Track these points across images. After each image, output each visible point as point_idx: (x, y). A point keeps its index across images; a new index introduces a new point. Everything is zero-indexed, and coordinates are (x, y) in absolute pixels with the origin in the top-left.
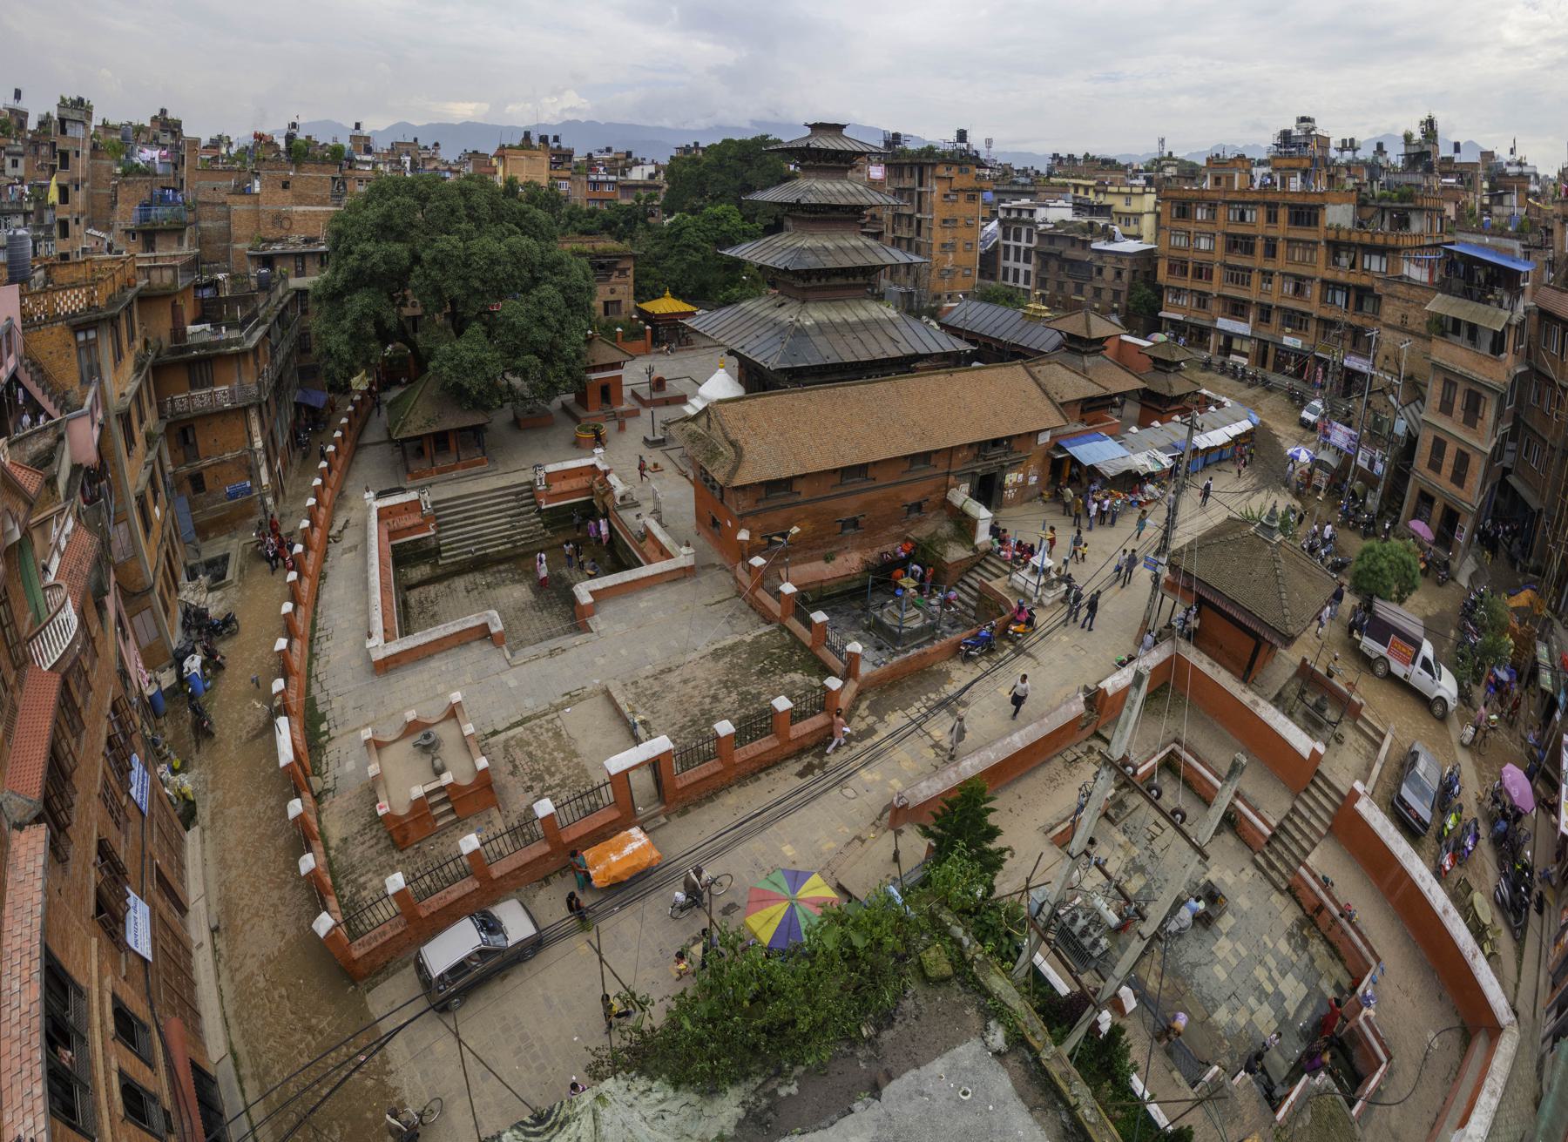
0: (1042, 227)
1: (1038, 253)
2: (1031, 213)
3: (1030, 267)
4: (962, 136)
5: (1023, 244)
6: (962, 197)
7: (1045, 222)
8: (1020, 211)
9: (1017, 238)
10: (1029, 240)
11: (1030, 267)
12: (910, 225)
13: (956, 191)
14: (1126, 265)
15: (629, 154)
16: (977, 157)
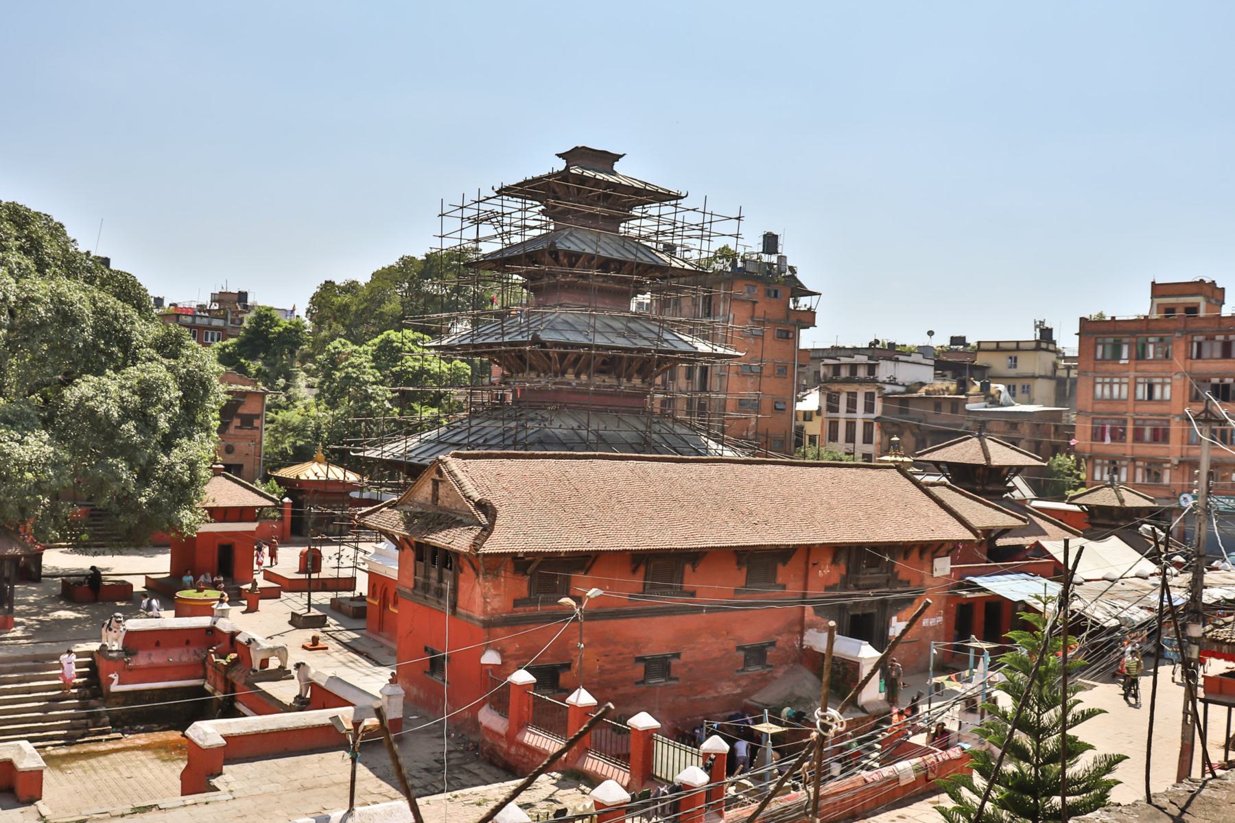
0: (888, 388)
1: (881, 428)
2: (872, 369)
3: (870, 449)
4: (771, 243)
5: (860, 414)
6: (770, 332)
7: (893, 381)
8: (854, 367)
9: (852, 406)
10: (869, 408)
12: (689, 375)
16: (793, 276)
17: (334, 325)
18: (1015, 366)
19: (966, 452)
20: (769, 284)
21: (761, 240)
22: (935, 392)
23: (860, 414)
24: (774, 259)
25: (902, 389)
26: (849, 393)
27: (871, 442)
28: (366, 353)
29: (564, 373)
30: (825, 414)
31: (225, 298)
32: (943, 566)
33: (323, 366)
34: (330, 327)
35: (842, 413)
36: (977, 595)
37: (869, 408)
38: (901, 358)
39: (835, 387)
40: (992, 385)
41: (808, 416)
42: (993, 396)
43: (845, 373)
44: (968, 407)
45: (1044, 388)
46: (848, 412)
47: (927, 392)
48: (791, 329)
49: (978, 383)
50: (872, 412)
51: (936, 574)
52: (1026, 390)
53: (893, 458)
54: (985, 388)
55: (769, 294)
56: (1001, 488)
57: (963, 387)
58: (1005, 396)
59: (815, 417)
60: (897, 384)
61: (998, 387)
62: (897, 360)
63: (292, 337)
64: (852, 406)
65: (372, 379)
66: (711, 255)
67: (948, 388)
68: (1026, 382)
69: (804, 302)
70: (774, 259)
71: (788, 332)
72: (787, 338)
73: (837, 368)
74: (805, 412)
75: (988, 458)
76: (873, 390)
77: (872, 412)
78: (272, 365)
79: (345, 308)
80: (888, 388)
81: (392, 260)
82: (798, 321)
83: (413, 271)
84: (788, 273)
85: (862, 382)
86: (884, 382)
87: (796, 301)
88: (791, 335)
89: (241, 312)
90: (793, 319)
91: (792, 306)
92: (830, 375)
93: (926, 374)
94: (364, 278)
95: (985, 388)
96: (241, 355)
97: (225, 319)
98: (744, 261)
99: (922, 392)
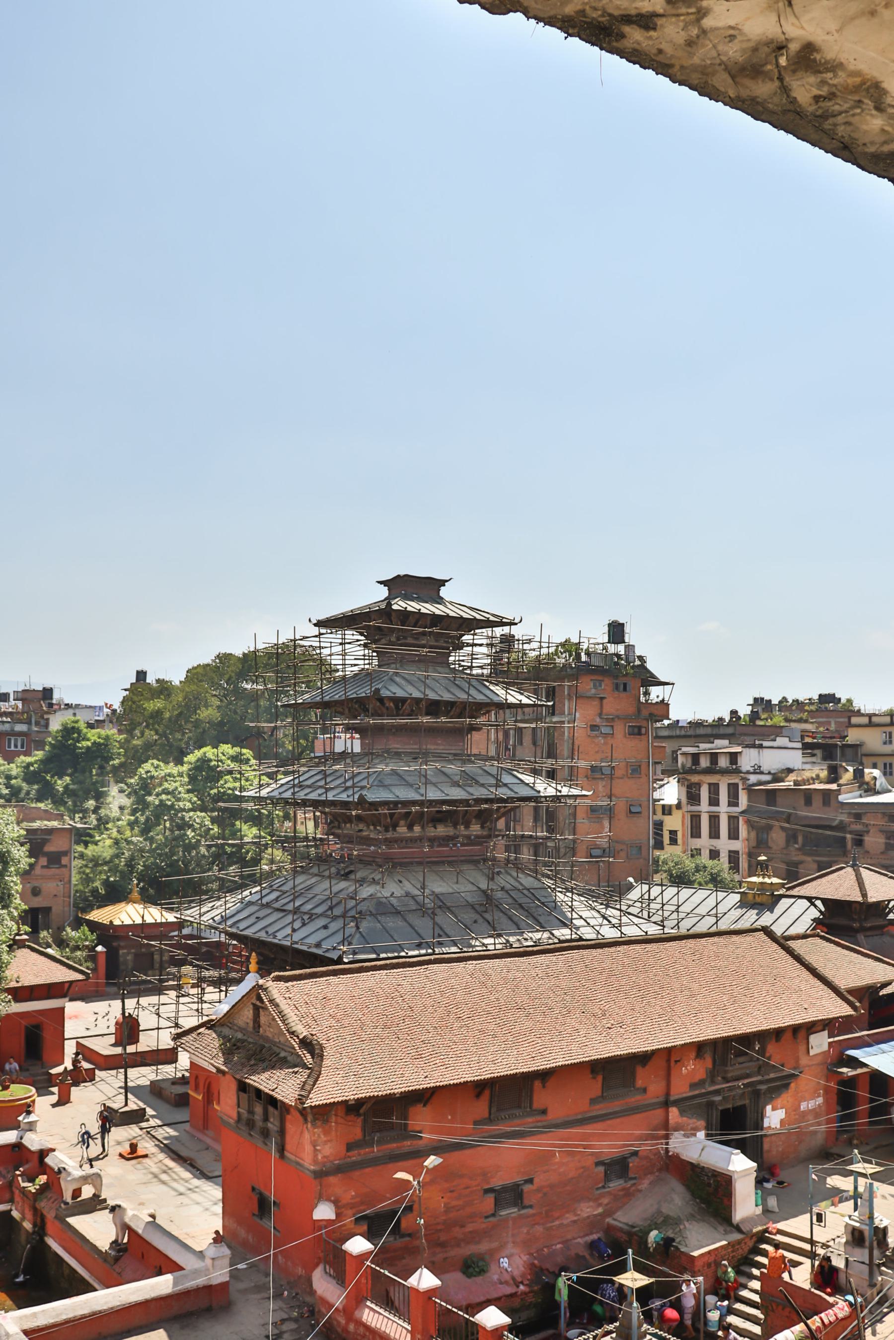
0: (753, 778)
1: (748, 822)
2: (734, 757)
3: (737, 845)
4: (616, 631)
5: (723, 809)
6: (620, 729)
7: (758, 771)
8: (714, 757)
9: (714, 801)
10: (733, 801)
11: (737, 845)
13: (611, 721)
16: (643, 667)
17: (147, 732)
18: (891, 742)
19: (840, 885)
20: (616, 677)
21: (606, 629)
23: (723, 809)
24: (621, 649)
26: (710, 784)
28: (181, 775)
29: (395, 826)
30: (686, 807)
31: (27, 695)
32: (820, 1043)
33: (135, 792)
34: (142, 734)
35: (704, 806)
36: (860, 1071)
37: (733, 801)
38: (765, 744)
39: (695, 778)
40: (867, 771)
41: (667, 810)
42: (867, 783)
43: (704, 763)
46: (710, 804)
47: (796, 783)
48: (644, 724)
49: (851, 769)
50: (736, 804)
51: (812, 1053)
53: (760, 880)
54: (859, 774)
55: (617, 687)
56: (879, 922)
57: (834, 775)
58: (881, 782)
59: (675, 811)
60: (762, 773)
61: (873, 773)
62: (761, 746)
63: (100, 752)
64: (714, 802)
65: (189, 805)
66: (552, 650)
67: (818, 776)
69: (656, 693)
70: (621, 649)
71: (640, 728)
72: (640, 734)
74: (663, 806)
75: (864, 895)
76: (736, 781)
77: (736, 804)
78: (80, 783)
79: (157, 715)
80: (753, 778)
81: (207, 657)
82: (651, 715)
83: (232, 670)
84: (637, 663)
85: (724, 772)
86: (748, 772)
87: (647, 693)
88: (643, 730)
89: (48, 713)
90: (645, 713)
91: (642, 699)
92: (689, 764)
93: (794, 758)
94: (177, 677)
95: (859, 774)
96: (46, 773)
97: (29, 723)
98: (588, 654)
99: (788, 783)
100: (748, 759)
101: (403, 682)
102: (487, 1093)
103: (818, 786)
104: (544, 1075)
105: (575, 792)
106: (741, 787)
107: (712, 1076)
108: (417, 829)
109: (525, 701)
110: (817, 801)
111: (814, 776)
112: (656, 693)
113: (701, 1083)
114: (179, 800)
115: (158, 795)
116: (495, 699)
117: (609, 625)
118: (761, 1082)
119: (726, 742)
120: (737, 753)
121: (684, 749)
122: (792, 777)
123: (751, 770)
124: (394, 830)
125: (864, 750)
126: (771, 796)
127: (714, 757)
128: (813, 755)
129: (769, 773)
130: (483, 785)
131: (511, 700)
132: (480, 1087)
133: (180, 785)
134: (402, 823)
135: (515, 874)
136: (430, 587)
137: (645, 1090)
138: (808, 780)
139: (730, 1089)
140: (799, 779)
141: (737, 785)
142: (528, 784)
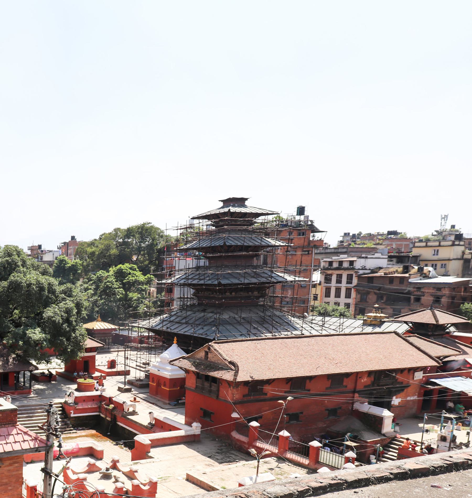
0: (361, 272)
2: (352, 263)
8: (341, 263)
14: (446, 292)
15: (40, 247)
22: (390, 273)
25: (369, 271)
27: (350, 298)
43: (335, 265)
44: (410, 280)
45: (456, 265)
48: (311, 249)
52: (444, 266)
60: (366, 269)
67: (397, 271)
68: (444, 262)
72: (308, 254)
73: (331, 263)
76: (352, 273)
86: (359, 269)
87: (313, 236)
88: (310, 252)
90: (312, 245)
91: (311, 239)
92: (327, 265)
99: (381, 273)
100: (359, 263)
101: (232, 239)
102: (290, 382)
103: (396, 275)
104: (311, 378)
105: (301, 279)
106: (354, 275)
107: (373, 384)
108: (233, 293)
109: (282, 244)
110: (396, 282)
111: (395, 270)
112: (318, 236)
113: (368, 386)
114: (113, 285)
115: (105, 283)
116: (270, 244)
117: (298, 208)
118: (392, 388)
119: (346, 256)
120: (353, 261)
121: (325, 259)
122: (381, 271)
123: (361, 268)
124: (225, 294)
125: (421, 258)
126: (371, 280)
127: (341, 263)
128: (392, 261)
129: (370, 269)
130: (263, 277)
131: (277, 244)
132: (289, 380)
133: (112, 279)
134: (228, 291)
135: (272, 311)
136: (241, 201)
137: (346, 386)
138: (392, 272)
139: (380, 389)
140: (387, 272)
141: (352, 275)
142: (281, 277)
